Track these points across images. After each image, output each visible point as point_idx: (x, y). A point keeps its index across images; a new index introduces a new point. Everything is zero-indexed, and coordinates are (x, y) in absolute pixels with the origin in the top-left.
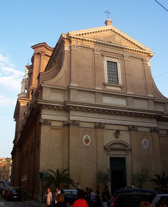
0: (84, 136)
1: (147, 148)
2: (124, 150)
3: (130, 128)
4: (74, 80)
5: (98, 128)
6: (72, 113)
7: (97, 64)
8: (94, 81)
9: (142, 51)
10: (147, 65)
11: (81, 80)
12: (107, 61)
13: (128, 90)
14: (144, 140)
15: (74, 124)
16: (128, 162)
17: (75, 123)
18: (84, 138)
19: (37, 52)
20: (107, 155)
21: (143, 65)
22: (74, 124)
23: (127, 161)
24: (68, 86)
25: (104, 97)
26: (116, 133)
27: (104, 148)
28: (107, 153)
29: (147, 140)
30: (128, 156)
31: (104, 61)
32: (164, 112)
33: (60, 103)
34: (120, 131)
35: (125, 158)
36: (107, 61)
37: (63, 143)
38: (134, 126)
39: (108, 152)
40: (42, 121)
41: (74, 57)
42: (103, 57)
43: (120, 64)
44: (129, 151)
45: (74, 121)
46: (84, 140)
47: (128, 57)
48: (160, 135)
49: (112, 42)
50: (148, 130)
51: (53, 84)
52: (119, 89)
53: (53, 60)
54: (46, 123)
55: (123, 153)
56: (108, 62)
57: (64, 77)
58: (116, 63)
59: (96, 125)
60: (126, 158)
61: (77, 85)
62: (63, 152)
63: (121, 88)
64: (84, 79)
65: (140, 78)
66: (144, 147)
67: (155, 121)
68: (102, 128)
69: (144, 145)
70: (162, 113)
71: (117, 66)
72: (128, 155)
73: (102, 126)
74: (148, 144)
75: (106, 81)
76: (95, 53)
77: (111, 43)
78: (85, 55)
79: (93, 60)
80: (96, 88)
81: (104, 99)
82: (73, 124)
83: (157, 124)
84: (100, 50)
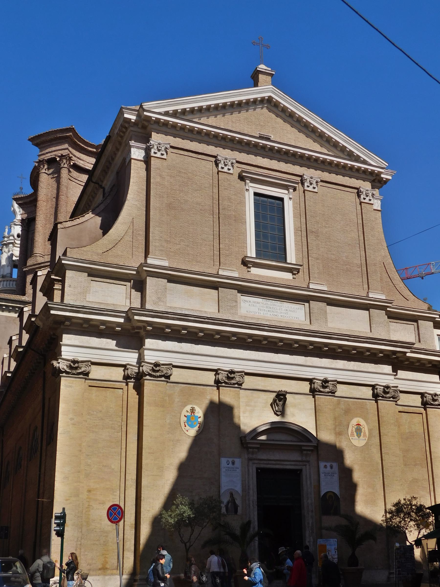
2: (299, 449)
4: (156, 246)
5: (223, 384)
8: (215, 252)
9: (357, 164)
10: (371, 206)
11: (178, 247)
12: (256, 194)
14: (354, 422)
15: (158, 374)
16: (309, 482)
17: (158, 371)
18: (184, 413)
19: (48, 156)
20: (251, 463)
21: (359, 208)
22: (158, 374)
23: (304, 477)
24: (141, 265)
26: (275, 401)
27: (242, 444)
28: (250, 456)
29: (365, 421)
30: (308, 467)
31: (247, 193)
32: (413, 344)
33: (115, 313)
34: (288, 396)
35: (301, 470)
36: (256, 194)
38: (325, 381)
39: (253, 453)
40: (62, 365)
41: (158, 179)
43: (291, 202)
44: (312, 451)
45: (157, 365)
46: (184, 419)
47: (317, 182)
48: (401, 408)
49: (272, 138)
50: (368, 393)
51: (95, 258)
52: (288, 276)
53: (97, 185)
54: (74, 372)
55: (295, 456)
56: (258, 198)
57: (128, 238)
58: (282, 200)
61: (165, 263)
63: (292, 273)
64: (188, 246)
65: (349, 245)
68: (236, 386)
70: (409, 345)
72: (308, 462)
73: (237, 379)
75: (251, 252)
76: (220, 169)
77: (268, 139)
78: (190, 175)
79: (216, 191)
80: (221, 272)
81: (242, 304)
82: (153, 373)
84: (234, 161)
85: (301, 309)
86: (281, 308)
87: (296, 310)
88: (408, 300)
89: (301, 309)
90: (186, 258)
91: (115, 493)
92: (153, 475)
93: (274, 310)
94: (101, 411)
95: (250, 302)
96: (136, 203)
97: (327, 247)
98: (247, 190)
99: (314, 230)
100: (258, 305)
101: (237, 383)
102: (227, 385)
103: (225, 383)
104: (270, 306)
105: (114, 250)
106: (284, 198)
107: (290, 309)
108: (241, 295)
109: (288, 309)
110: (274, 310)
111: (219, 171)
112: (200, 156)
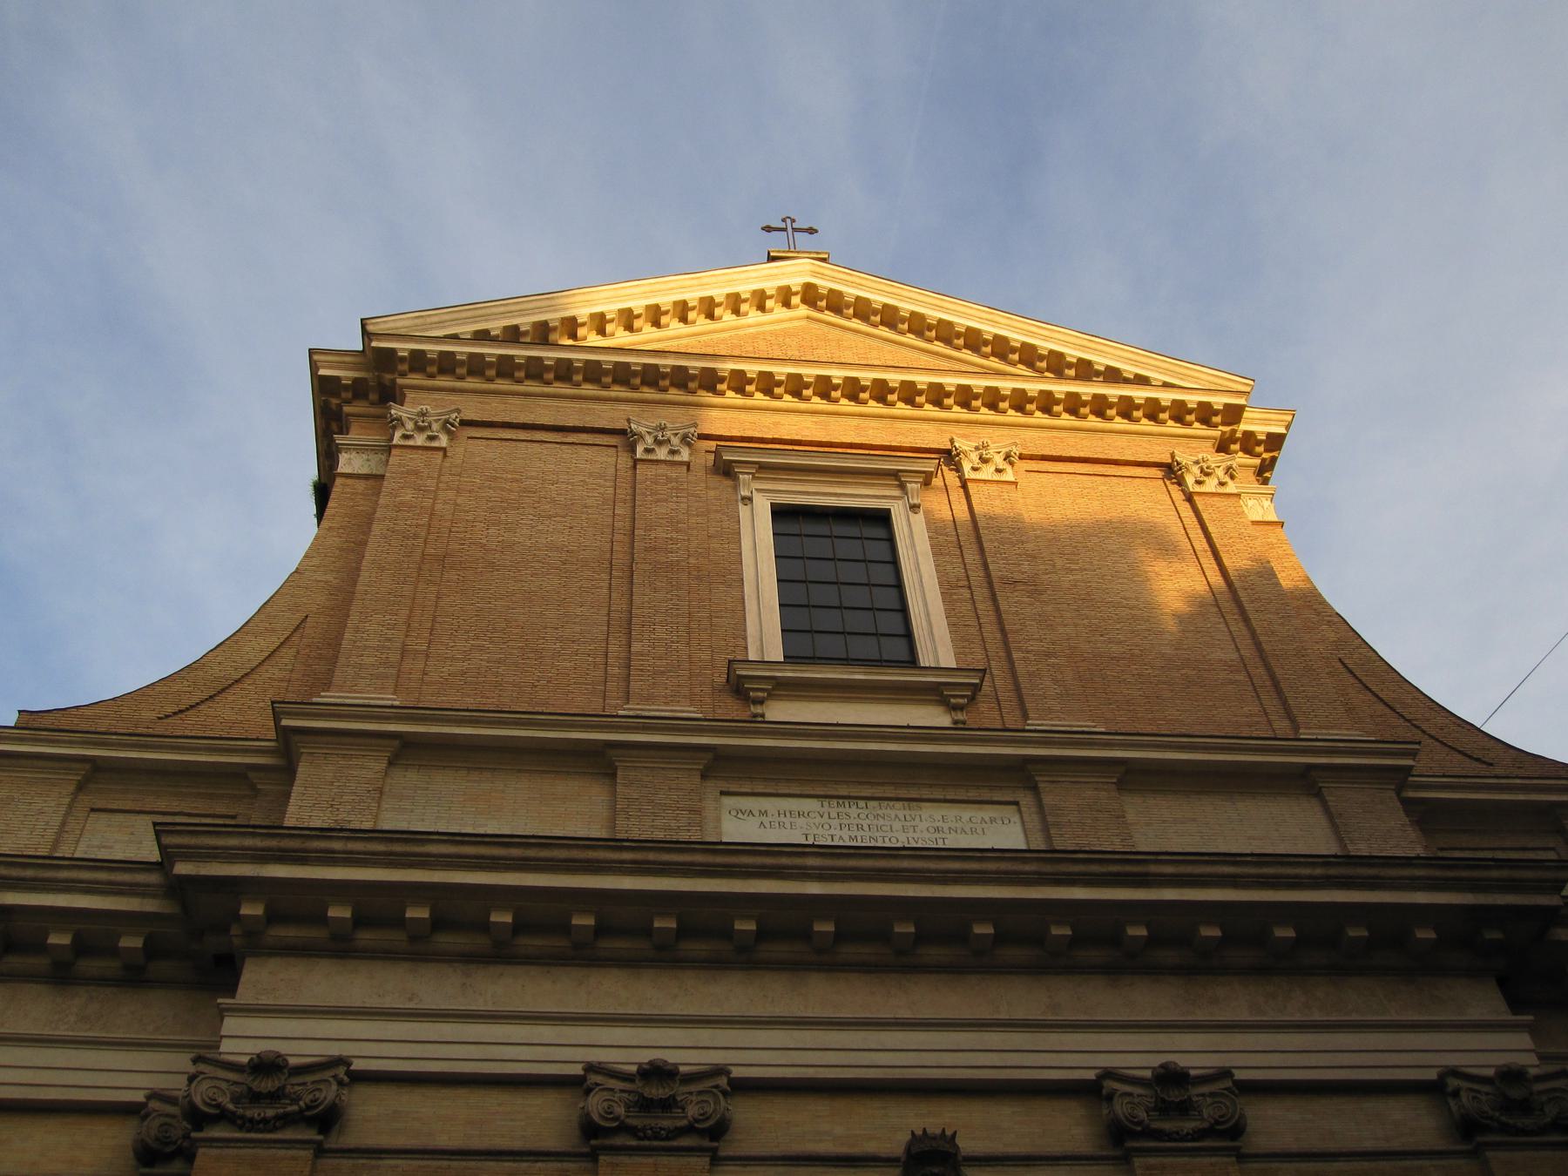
3: (1121, 1108)
6: (257, 980)
7: (661, 533)
13: (1050, 710)
25: (729, 802)
31: (744, 511)
36: (781, 513)
42: (729, 483)
45: (266, 1066)
52: (932, 716)
58: (882, 518)
59: (595, 1104)
67: (1486, 1003)
71: (891, 540)
82: (254, 1112)
83: (1524, 1040)
85: (1006, 821)
86: (913, 823)
87: (984, 825)
88: (1491, 764)
89: (1006, 821)
90: (488, 698)
93: (877, 834)
95: (764, 813)
96: (329, 577)
97: (1085, 621)
98: (743, 498)
99: (1017, 577)
100: (801, 821)
101: (690, 1130)
102: (634, 1143)
103: (632, 1131)
104: (860, 822)
105: (210, 707)
106: (890, 509)
107: (953, 825)
108: (723, 793)
109: (946, 827)
110: (877, 834)
111: (636, 462)
112: (572, 438)
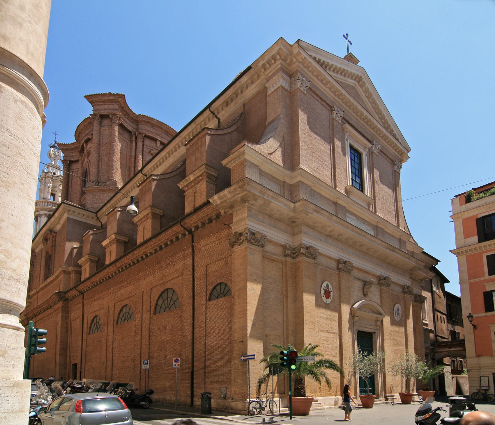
0: (323, 282)
1: (399, 319)
14: (396, 306)
18: (323, 287)
37: (284, 293)
46: (323, 292)
60: (376, 333)
62: (285, 311)
66: (396, 318)
69: (395, 315)
74: (401, 312)
91: (281, 339)
92: (310, 328)
94: (270, 277)
